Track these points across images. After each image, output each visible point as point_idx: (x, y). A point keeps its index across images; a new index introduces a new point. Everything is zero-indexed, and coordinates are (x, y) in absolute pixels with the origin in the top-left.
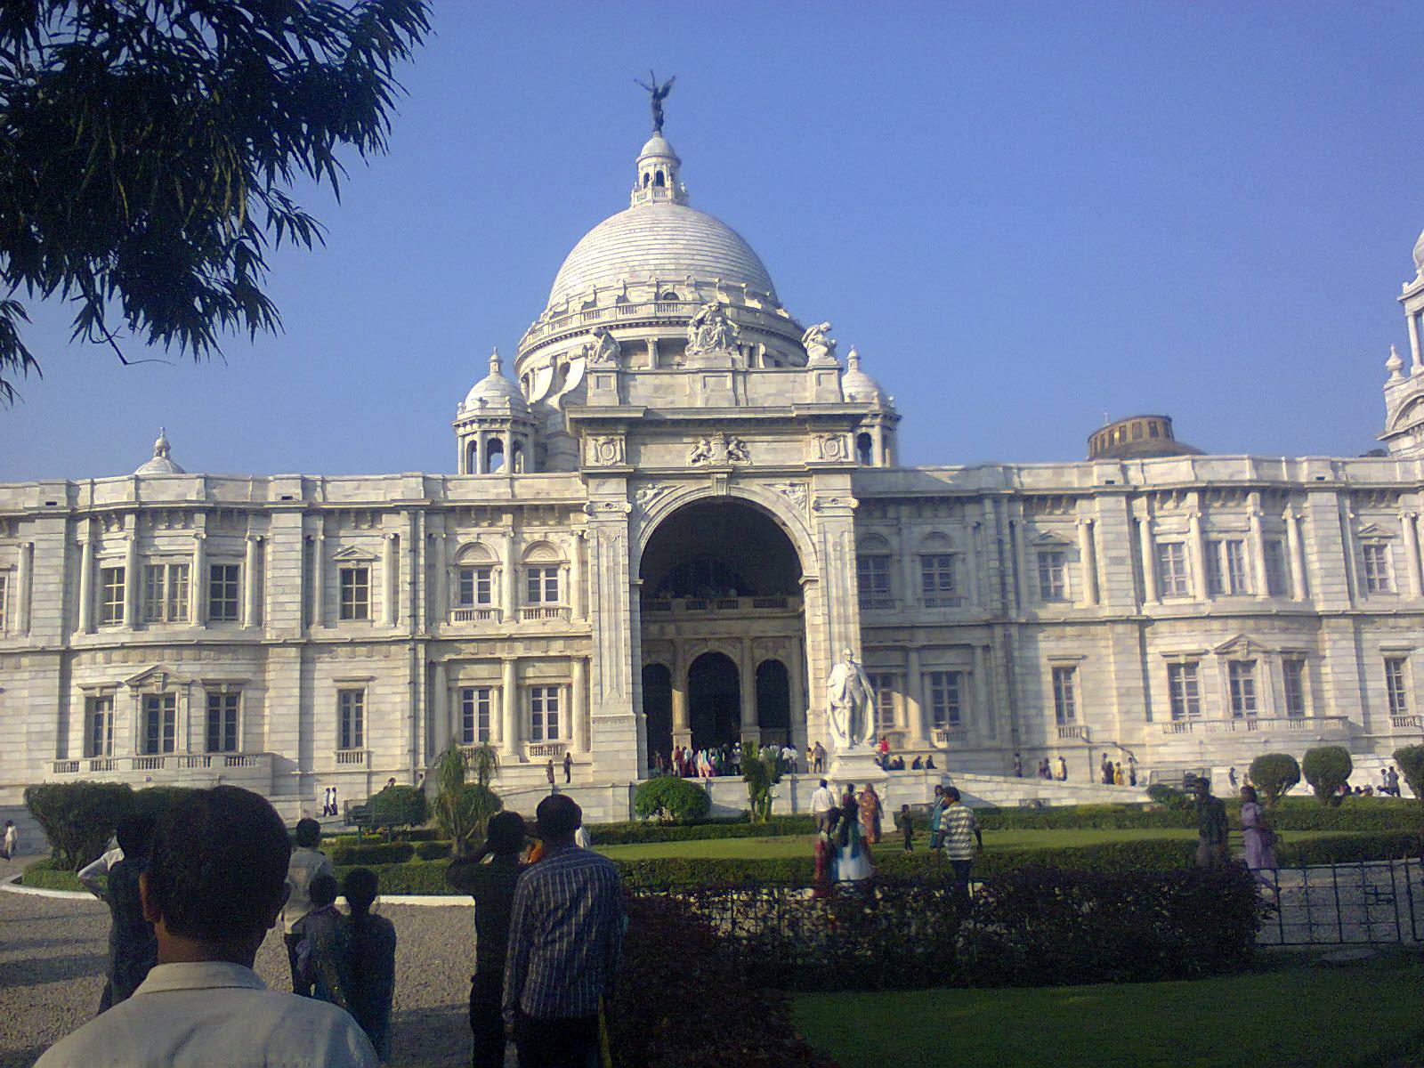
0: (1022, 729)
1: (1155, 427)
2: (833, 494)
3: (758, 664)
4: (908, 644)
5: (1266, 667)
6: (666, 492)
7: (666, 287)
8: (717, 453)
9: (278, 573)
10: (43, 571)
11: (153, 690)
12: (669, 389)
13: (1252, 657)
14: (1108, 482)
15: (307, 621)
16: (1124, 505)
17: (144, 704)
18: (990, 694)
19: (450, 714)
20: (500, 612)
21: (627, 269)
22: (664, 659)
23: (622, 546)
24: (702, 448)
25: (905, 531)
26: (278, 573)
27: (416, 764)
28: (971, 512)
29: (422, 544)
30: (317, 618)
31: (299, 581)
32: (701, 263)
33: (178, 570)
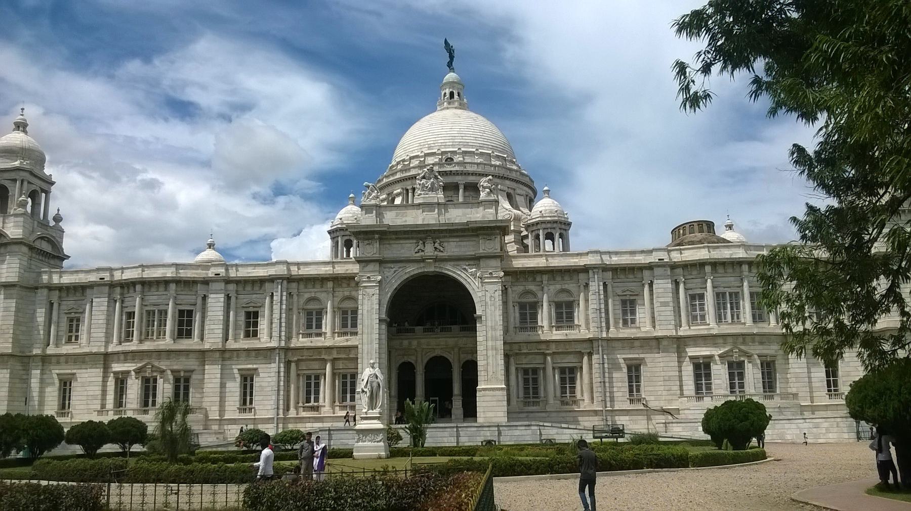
0: (608, 399)
1: (702, 227)
3: (462, 363)
5: (750, 365)
6: (401, 269)
7: (446, 155)
8: (429, 250)
13: (742, 359)
15: (226, 339)
16: (669, 273)
17: (142, 382)
21: (427, 146)
22: (412, 359)
23: (375, 299)
24: (421, 246)
25: (546, 289)
27: (278, 414)
28: (582, 276)
29: (284, 298)
31: (221, 318)
32: (467, 141)
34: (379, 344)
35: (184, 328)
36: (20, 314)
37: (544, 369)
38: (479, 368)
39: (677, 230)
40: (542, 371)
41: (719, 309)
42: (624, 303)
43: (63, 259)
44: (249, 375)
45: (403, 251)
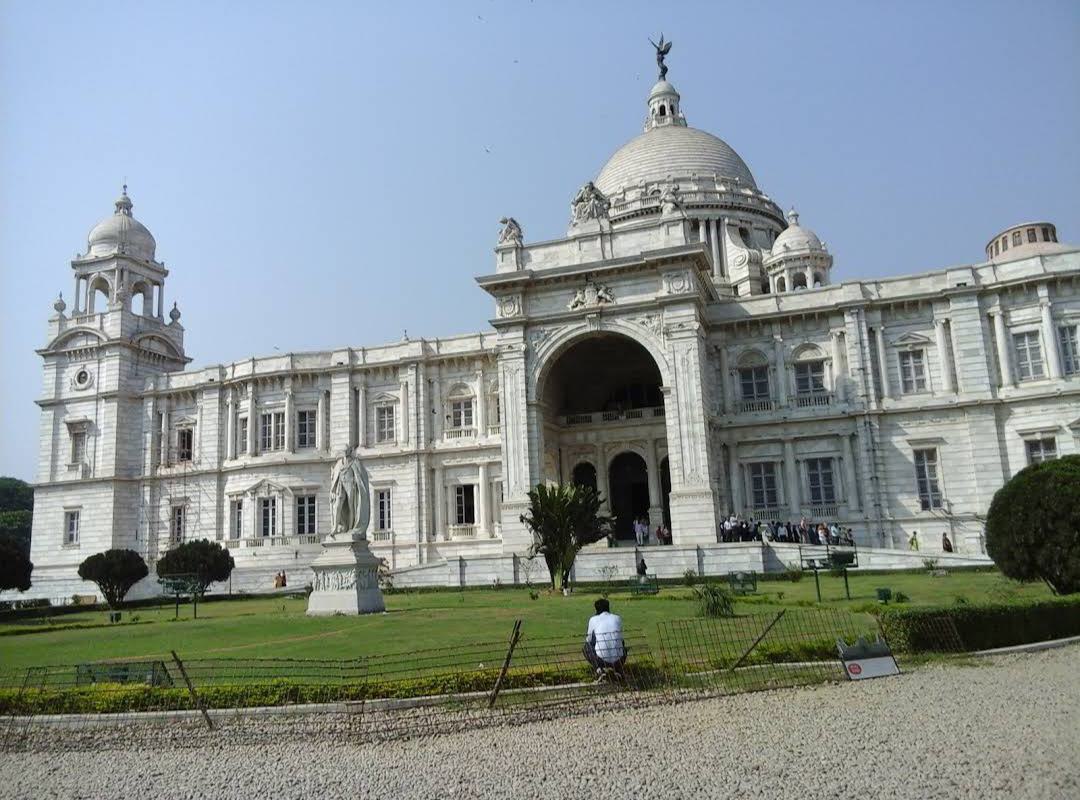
0: (884, 504)
2: (680, 320)
4: (782, 438)
8: (590, 299)
9: (337, 413)
10: (209, 422)
11: (263, 494)
12: (554, 256)
14: (958, 285)
17: (259, 505)
18: (856, 474)
19: (447, 503)
20: (476, 431)
22: (590, 459)
23: (521, 374)
26: (337, 413)
29: (421, 387)
30: (360, 443)
31: (348, 418)
33: (279, 416)
34: (529, 439)
35: (304, 439)
36: (125, 431)
37: (783, 463)
38: (673, 465)
39: (993, 244)
40: (779, 467)
41: (1066, 353)
42: (904, 356)
43: (184, 363)
44: (385, 490)
45: (556, 306)
